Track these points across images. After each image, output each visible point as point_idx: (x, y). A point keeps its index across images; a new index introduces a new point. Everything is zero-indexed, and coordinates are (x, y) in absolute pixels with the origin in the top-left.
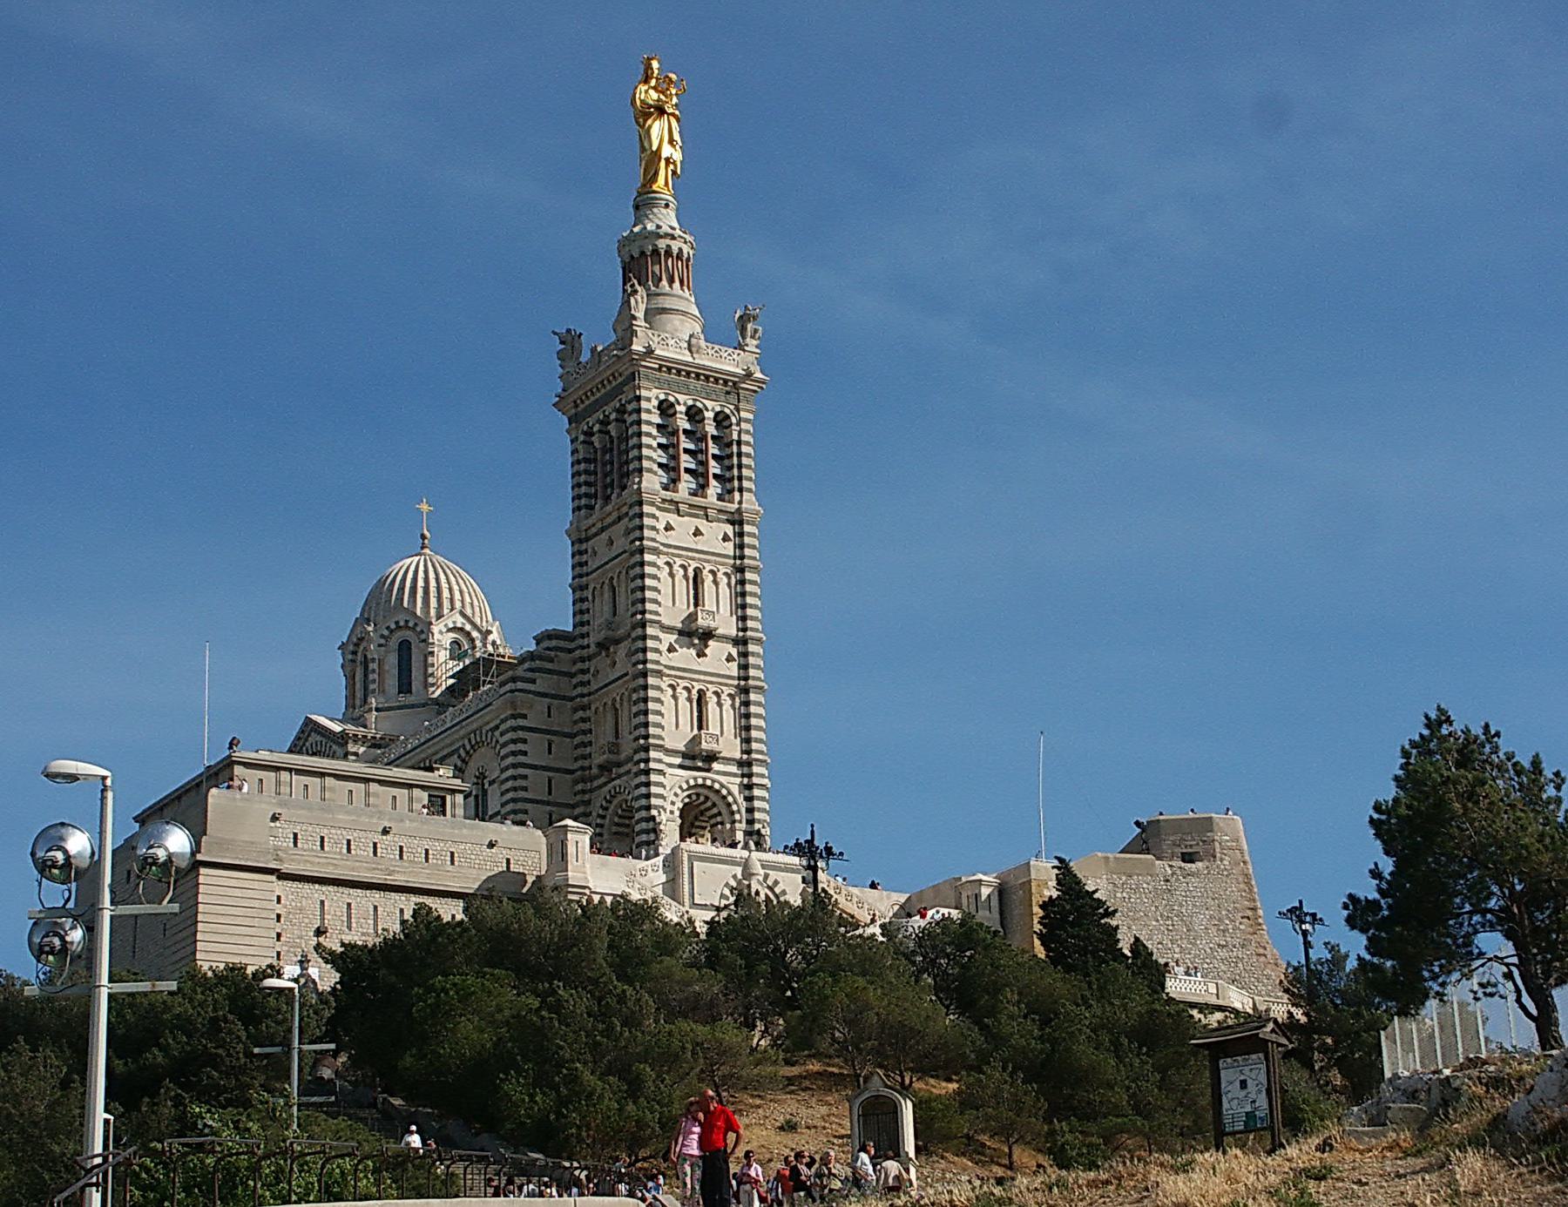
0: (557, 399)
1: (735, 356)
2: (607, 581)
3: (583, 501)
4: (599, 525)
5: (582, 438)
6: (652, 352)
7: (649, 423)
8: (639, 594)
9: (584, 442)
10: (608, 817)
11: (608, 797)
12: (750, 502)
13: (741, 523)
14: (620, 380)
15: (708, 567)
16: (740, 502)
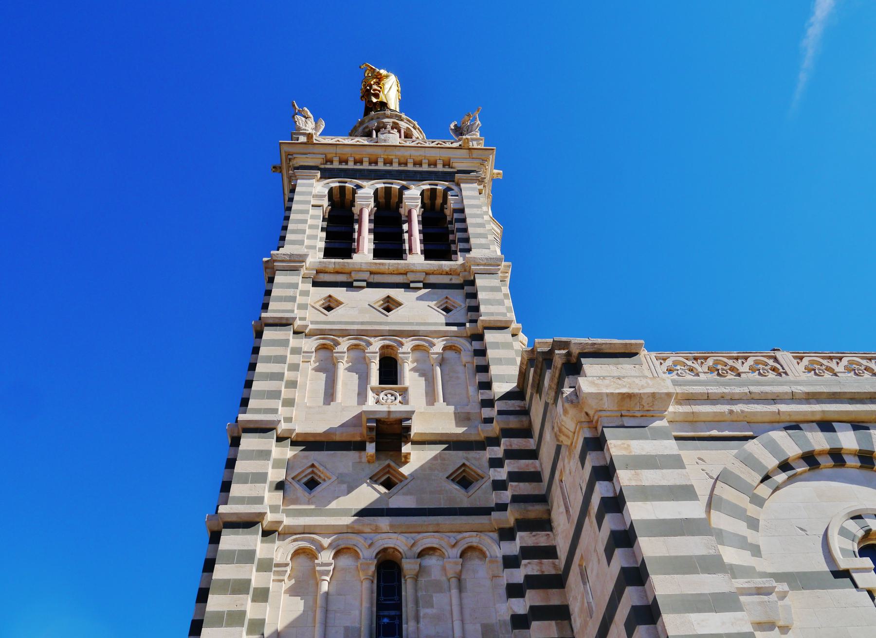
13: (472, 283)
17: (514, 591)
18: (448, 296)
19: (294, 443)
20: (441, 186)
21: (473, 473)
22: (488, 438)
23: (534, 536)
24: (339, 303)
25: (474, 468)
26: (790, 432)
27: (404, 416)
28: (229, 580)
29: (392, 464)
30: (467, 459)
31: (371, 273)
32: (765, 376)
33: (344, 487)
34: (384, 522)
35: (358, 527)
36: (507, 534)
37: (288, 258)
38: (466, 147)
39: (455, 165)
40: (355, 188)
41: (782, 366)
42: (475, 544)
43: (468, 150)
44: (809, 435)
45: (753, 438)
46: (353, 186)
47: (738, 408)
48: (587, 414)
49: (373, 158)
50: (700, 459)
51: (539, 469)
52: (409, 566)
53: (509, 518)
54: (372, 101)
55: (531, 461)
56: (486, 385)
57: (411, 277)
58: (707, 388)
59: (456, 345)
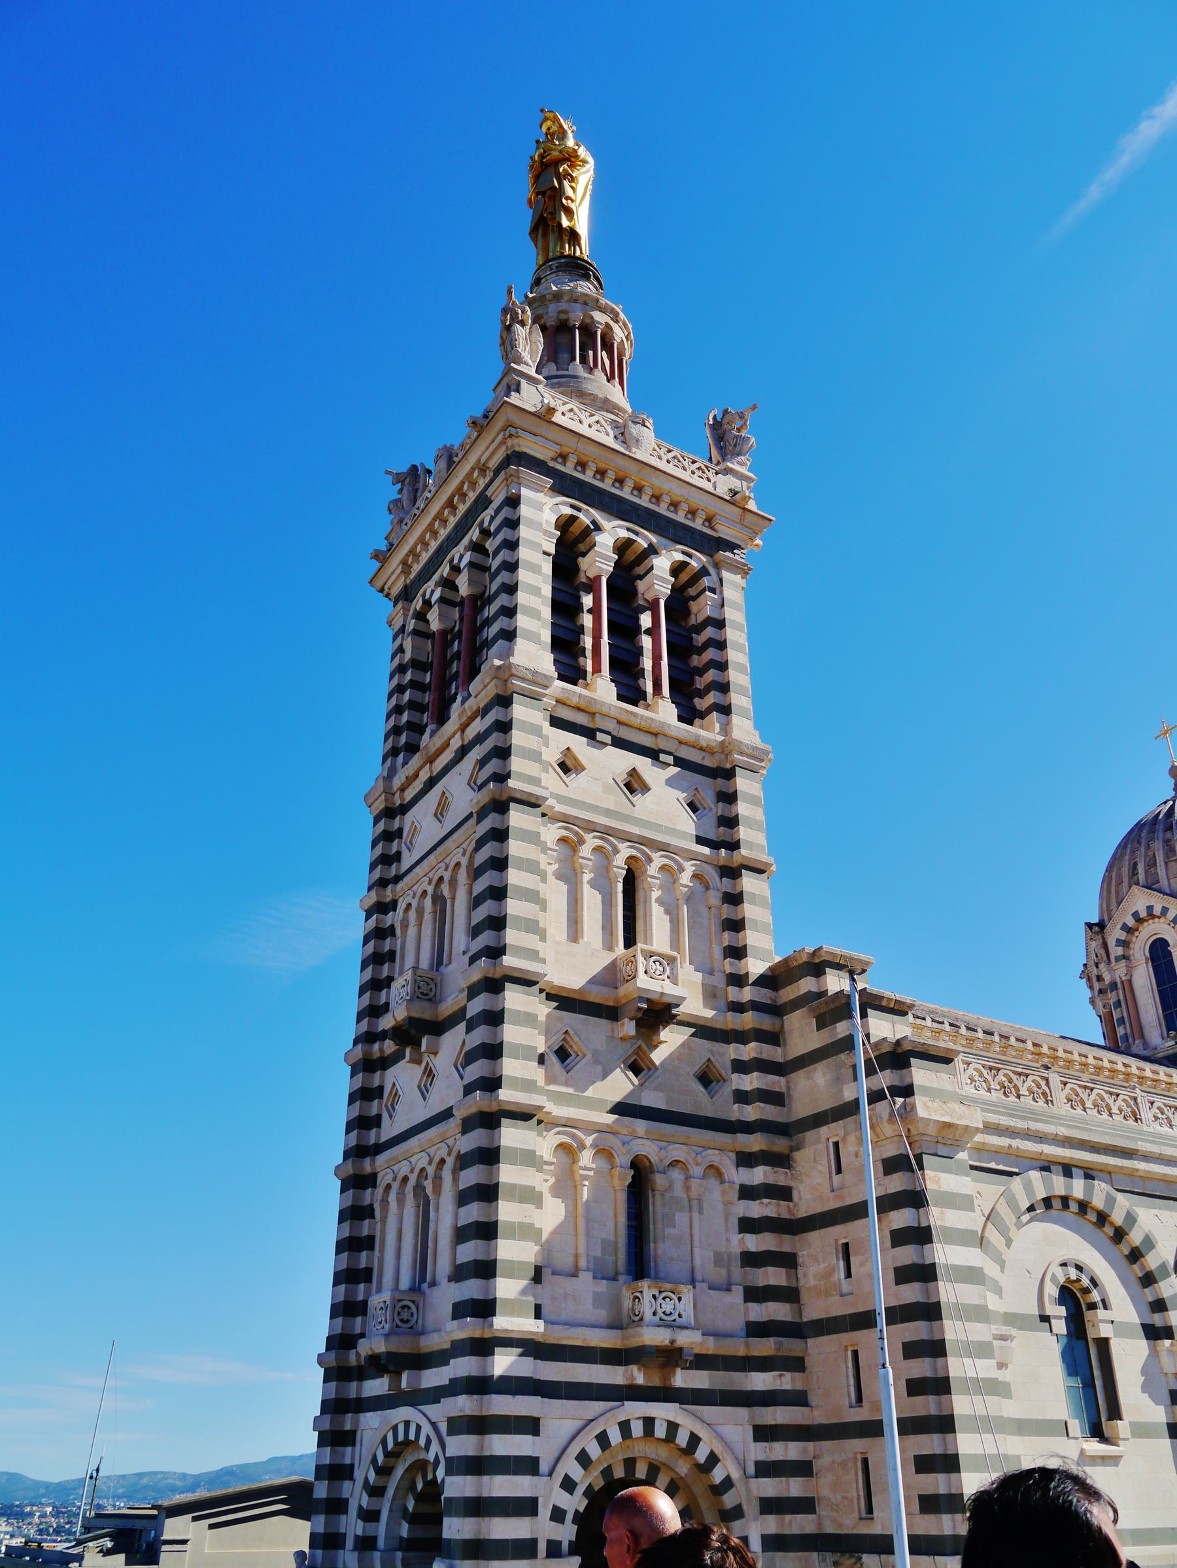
0: (377, 565)
1: (711, 474)
2: (430, 890)
3: (403, 739)
4: (424, 775)
5: (411, 624)
6: (551, 411)
7: (534, 545)
8: (487, 909)
9: (415, 632)
10: (390, 1493)
11: (380, 1459)
12: (743, 729)
13: (729, 774)
14: (482, 483)
15: (658, 859)
16: (726, 729)
17: (748, 1225)
18: (699, 789)
19: (550, 997)
20: (697, 560)
21: (715, 1071)
22: (735, 1031)
23: (775, 1172)
24: (583, 769)
25: (718, 1066)
26: (1043, 1173)
27: (675, 1001)
28: (515, 1185)
29: (644, 1047)
30: (712, 1052)
31: (619, 722)
32: (1037, 1102)
33: (599, 1068)
34: (641, 1126)
35: (617, 1128)
36: (746, 1160)
37: (530, 677)
38: (741, 505)
39: (718, 527)
40: (592, 527)
41: (1051, 1092)
42: (715, 1164)
43: (741, 511)
44: (1054, 1177)
45: (1017, 1174)
46: (588, 522)
47: (1017, 1143)
48: (909, 1130)
49: (621, 474)
50: (979, 1193)
51: (784, 1090)
52: (660, 1180)
53: (755, 1143)
54: (560, 225)
55: (777, 1078)
56: (737, 952)
57: (662, 744)
58: (1000, 1117)
59: (705, 876)
